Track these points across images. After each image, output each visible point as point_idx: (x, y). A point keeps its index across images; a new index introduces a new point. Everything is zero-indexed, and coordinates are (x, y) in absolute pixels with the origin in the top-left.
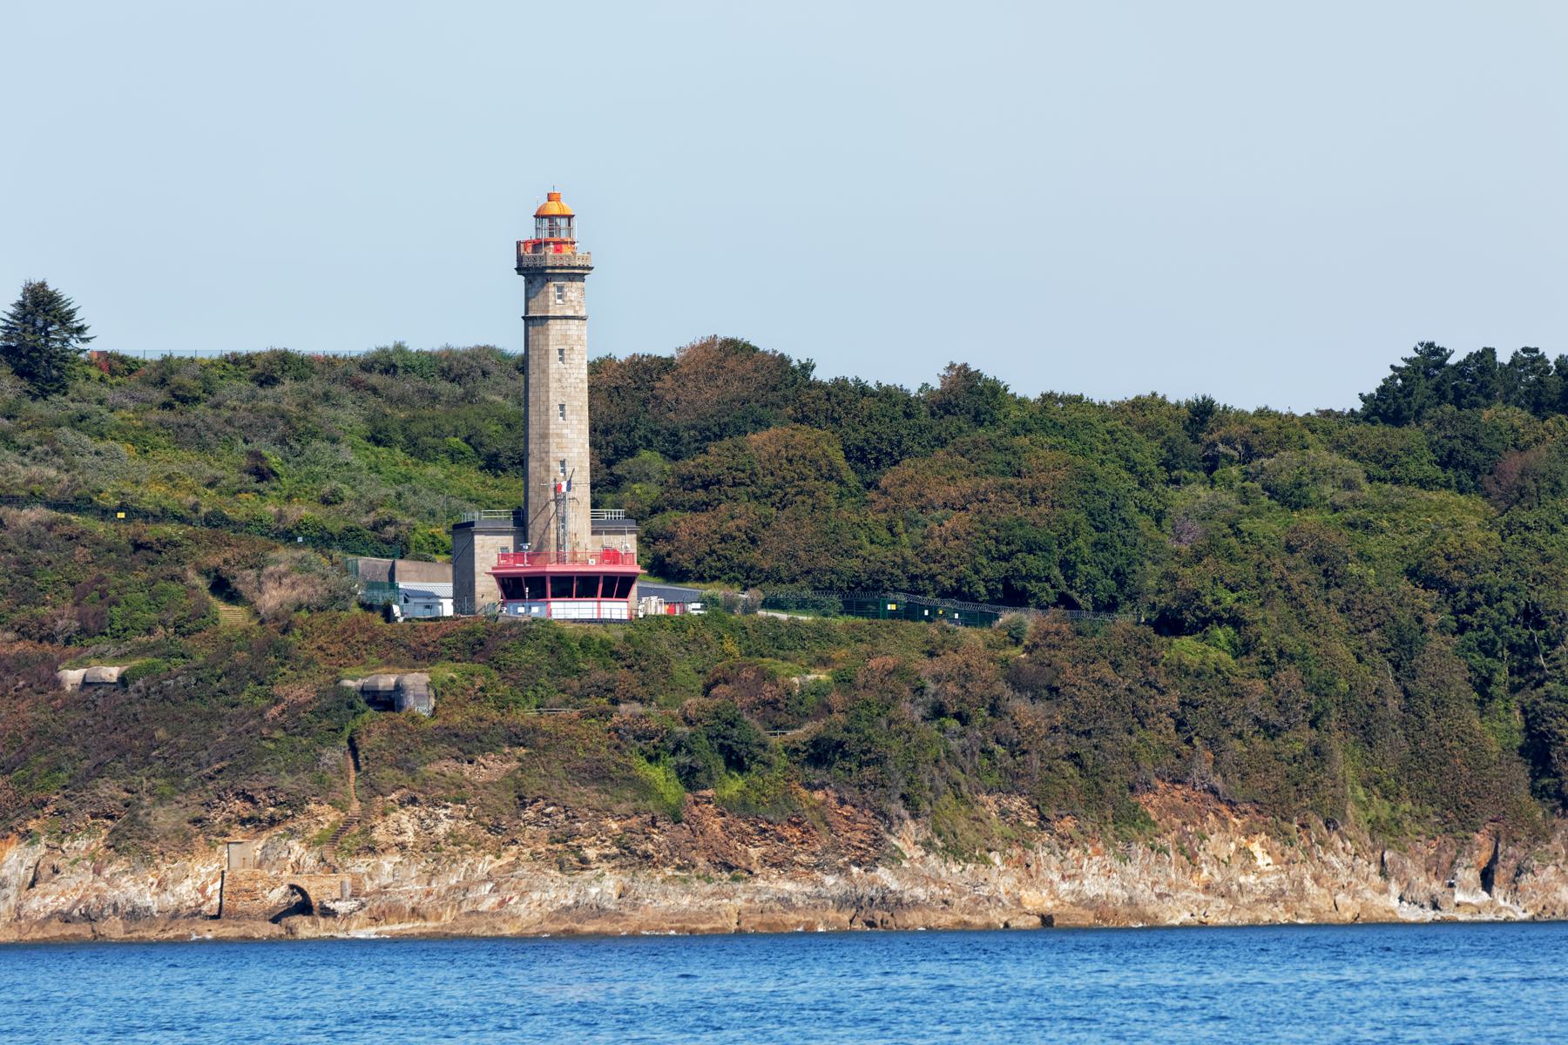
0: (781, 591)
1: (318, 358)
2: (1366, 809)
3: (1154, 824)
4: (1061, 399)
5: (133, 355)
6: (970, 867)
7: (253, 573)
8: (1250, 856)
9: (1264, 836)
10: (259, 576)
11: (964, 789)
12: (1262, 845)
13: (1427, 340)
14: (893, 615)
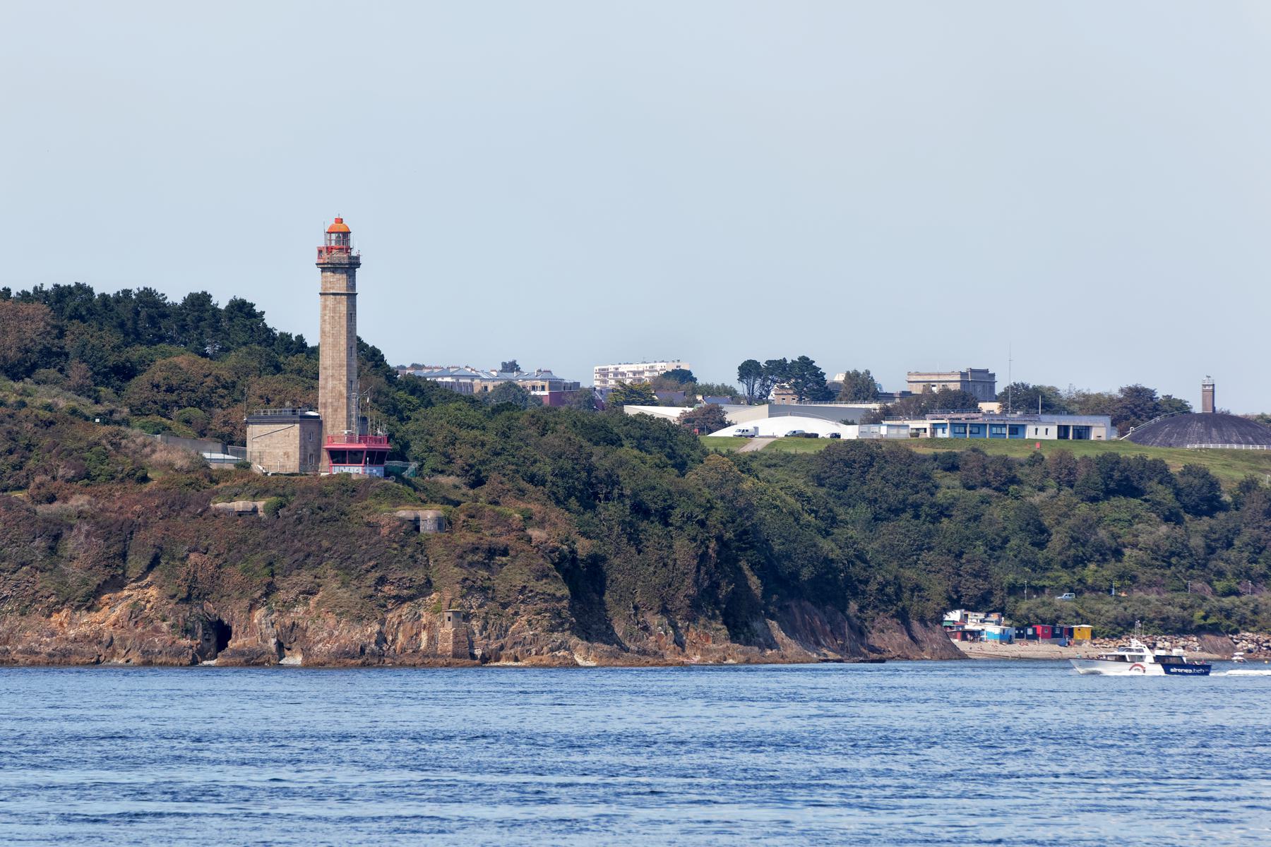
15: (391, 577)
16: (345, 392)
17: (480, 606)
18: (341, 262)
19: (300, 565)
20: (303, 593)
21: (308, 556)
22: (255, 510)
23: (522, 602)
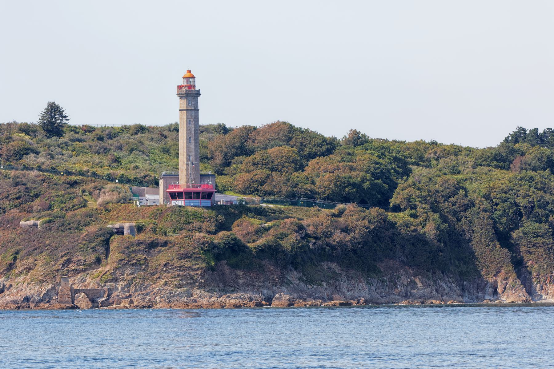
0: (270, 198)
1: (151, 127)
2: (458, 268)
3: (382, 272)
4: (398, 142)
5: (93, 126)
6: (315, 287)
7: (98, 191)
8: (415, 283)
9: (420, 277)
11: (315, 261)
12: (419, 279)
13: (520, 126)
15: (74, 259)
16: (185, 161)
17: (131, 274)
18: (190, 94)
19: (29, 254)
20: (26, 268)
21: (36, 249)
22: (35, 225)
23: (165, 271)
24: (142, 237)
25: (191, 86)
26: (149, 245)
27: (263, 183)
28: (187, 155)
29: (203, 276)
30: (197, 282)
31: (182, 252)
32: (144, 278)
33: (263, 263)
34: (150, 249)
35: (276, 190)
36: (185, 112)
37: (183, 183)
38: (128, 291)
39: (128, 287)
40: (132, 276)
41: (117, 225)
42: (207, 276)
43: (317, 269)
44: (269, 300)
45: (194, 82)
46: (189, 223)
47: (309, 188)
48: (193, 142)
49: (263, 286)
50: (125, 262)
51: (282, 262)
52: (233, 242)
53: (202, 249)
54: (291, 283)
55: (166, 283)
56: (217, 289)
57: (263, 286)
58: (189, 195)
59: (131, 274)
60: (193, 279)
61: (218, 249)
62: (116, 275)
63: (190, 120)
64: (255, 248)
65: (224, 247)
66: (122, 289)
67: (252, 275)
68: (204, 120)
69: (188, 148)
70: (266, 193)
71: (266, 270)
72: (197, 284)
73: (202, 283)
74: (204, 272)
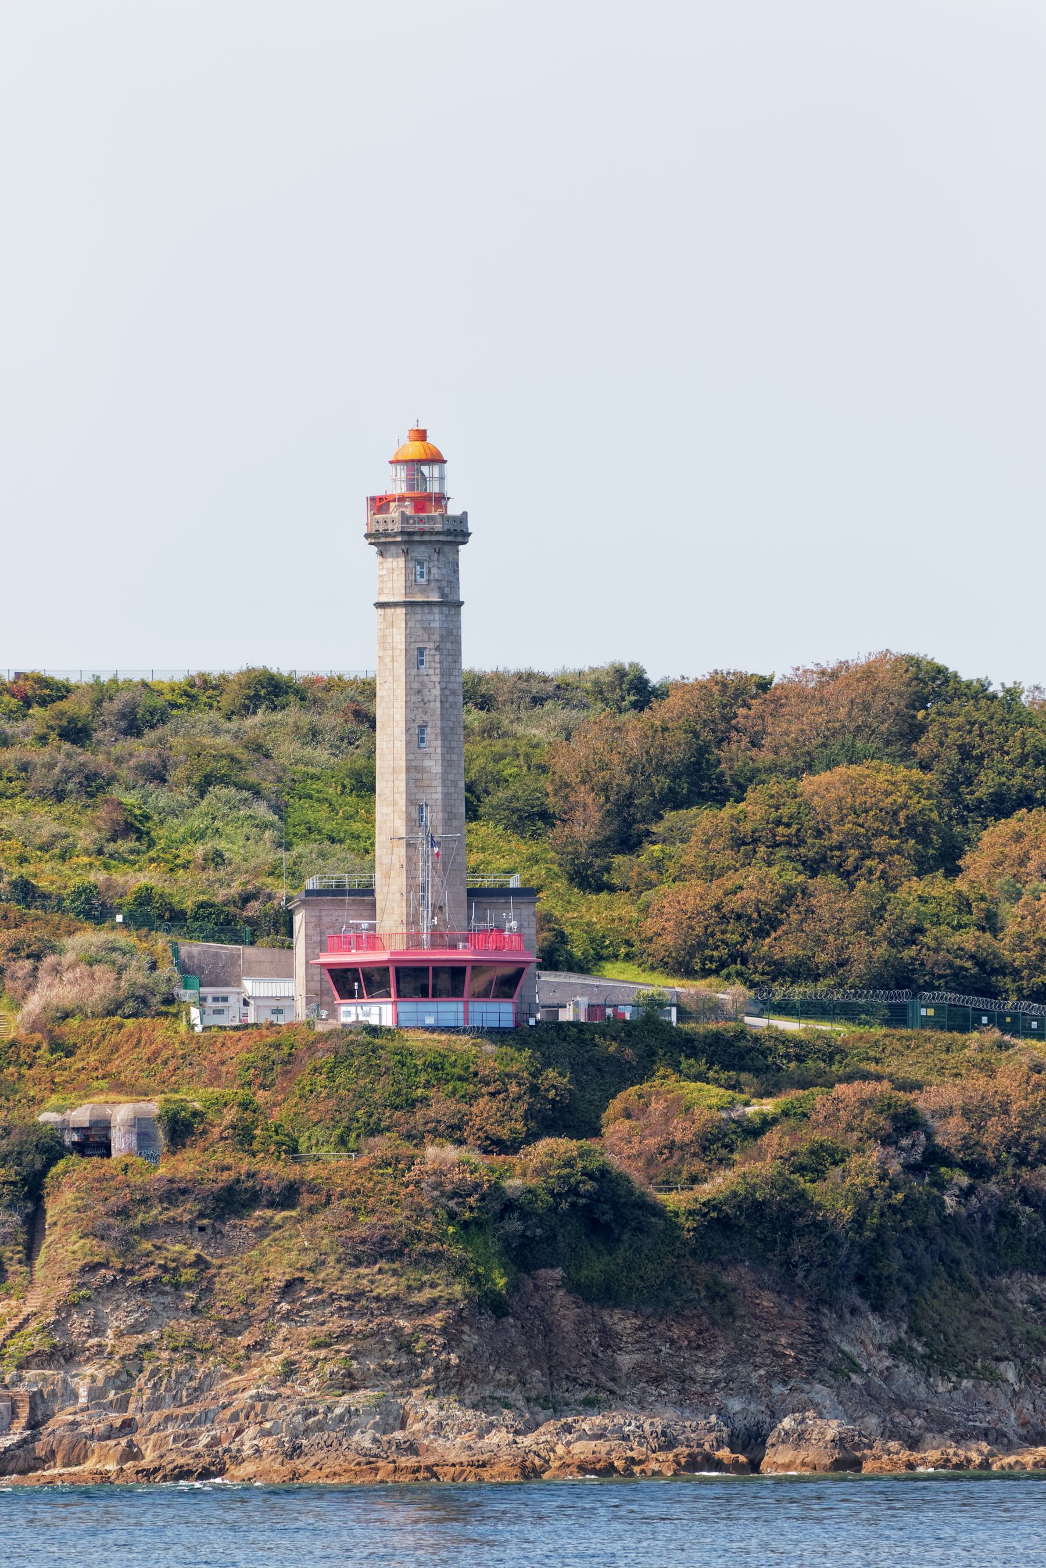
0: (799, 992)
1: (319, 680)
5: (59, 677)
6: (967, 1384)
7: (28, 964)
10: (36, 969)
11: (968, 1271)
14: (926, 1022)
16: (402, 832)
17: (135, 1329)
18: (425, 535)
23: (287, 1317)
24: (186, 1164)
25: (428, 498)
26: (217, 1199)
27: (767, 924)
28: (411, 801)
29: (451, 1336)
30: (425, 1364)
31: (360, 1231)
32: (192, 1349)
33: (729, 1278)
34: (221, 1218)
35: (823, 958)
36: (401, 611)
37: (393, 926)
38: (122, 1405)
39: (118, 1389)
40: (141, 1338)
41: (81, 1115)
42: (471, 1339)
43: (975, 1306)
44: (751, 1442)
45: (442, 478)
46: (412, 1104)
47: (970, 947)
48: (434, 745)
49: (729, 1380)
50: (110, 1275)
51: (813, 1276)
52: (589, 1186)
53: (452, 1216)
54: (855, 1368)
55: (290, 1369)
56: (516, 1396)
57: (729, 1380)
58: (414, 980)
59: (135, 1329)
60: (410, 1352)
61: (525, 1216)
62: (66, 1333)
63: (421, 651)
64: (691, 1213)
65: (553, 1209)
66: (96, 1395)
67: (676, 1332)
68: (487, 649)
69: (414, 770)
70: (780, 971)
71: (741, 1311)
72: (428, 1373)
73: (448, 1367)
74: (460, 1318)
